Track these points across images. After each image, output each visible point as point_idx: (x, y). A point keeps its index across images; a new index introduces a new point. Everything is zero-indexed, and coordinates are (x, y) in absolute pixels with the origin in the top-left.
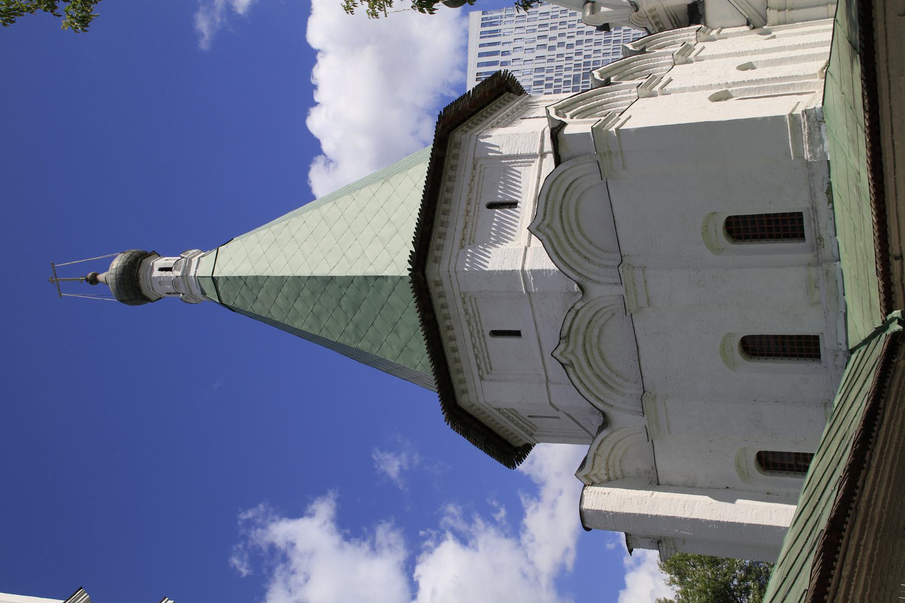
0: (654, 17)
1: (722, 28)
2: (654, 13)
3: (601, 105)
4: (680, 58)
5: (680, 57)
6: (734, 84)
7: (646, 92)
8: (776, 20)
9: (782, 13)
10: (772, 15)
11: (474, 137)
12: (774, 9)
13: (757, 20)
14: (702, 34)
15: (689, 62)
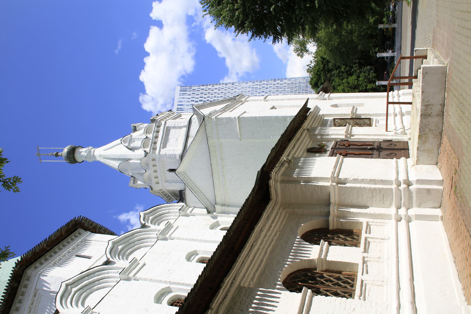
0: (162, 193)
1: (195, 207)
2: (162, 191)
3: (99, 280)
4: (161, 237)
5: (161, 236)
6: (174, 283)
7: (124, 277)
8: (220, 211)
9: (223, 207)
10: (218, 208)
11: (38, 275)
12: (220, 205)
13: (211, 209)
14: (182, 212)
15: (165, 239)
